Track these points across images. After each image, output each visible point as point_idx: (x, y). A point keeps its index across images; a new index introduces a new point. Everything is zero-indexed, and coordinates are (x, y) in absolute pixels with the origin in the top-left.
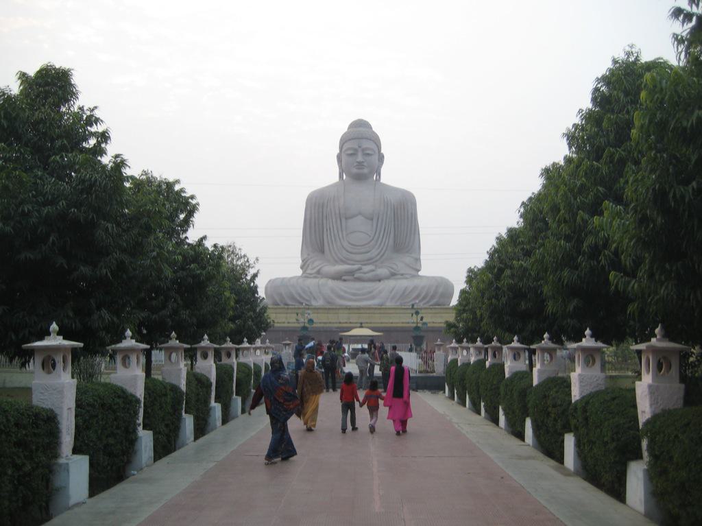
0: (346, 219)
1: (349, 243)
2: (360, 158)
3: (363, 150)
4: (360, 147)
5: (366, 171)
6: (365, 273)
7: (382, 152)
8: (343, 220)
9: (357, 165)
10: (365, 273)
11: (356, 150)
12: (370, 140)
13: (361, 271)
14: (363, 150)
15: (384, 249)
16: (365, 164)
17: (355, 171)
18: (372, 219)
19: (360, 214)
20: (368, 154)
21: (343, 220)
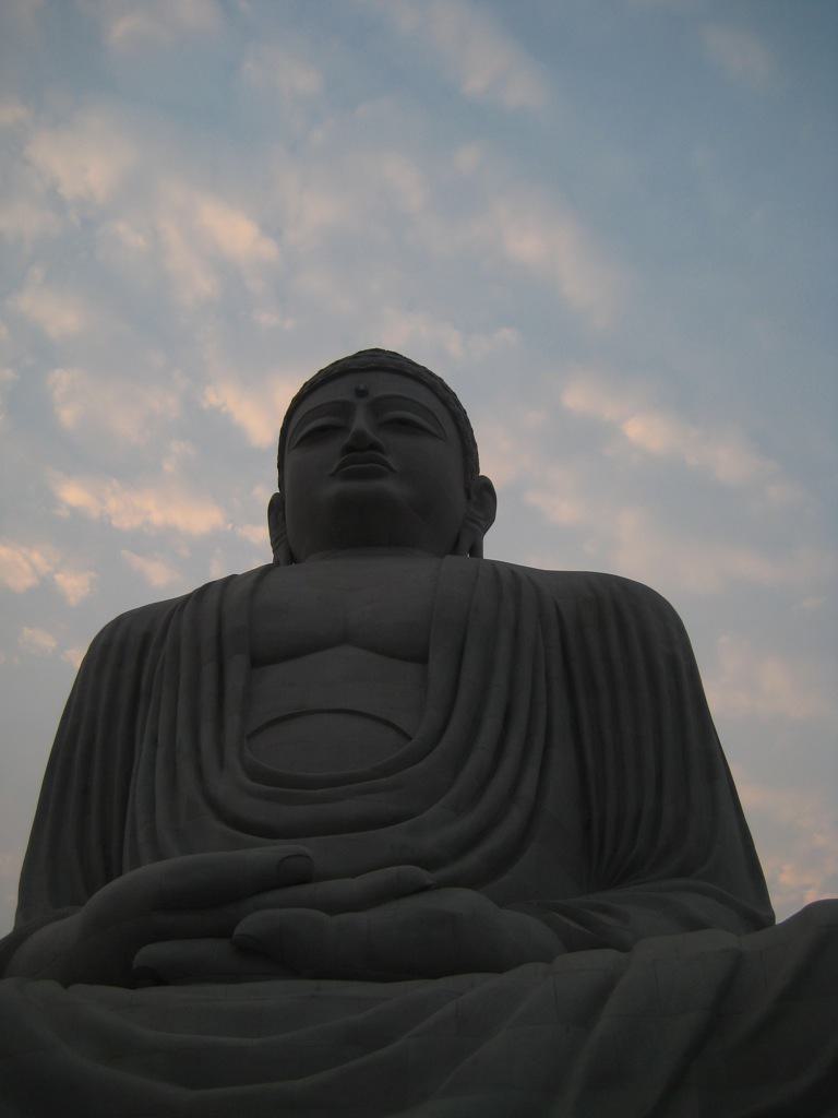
0: (257, 662)
1: (255, 774)
2: (361, 422)
3: (377, 407)
4: (361, 393)
5: (390, 486)
6: (333, 907)
7: (485, 469)
8: (237, 665)
9: (342, 465)
10: (333, 907)
11: (345, 409)
12: (424, 383)
13: (304, 891)
14: (377, 407)
15: (516, 817)
16: (389, 459)
17: (335, 488)
18: (422, 659)
19: (345, 638)
20: (403, 425)
21: (237, 665)
